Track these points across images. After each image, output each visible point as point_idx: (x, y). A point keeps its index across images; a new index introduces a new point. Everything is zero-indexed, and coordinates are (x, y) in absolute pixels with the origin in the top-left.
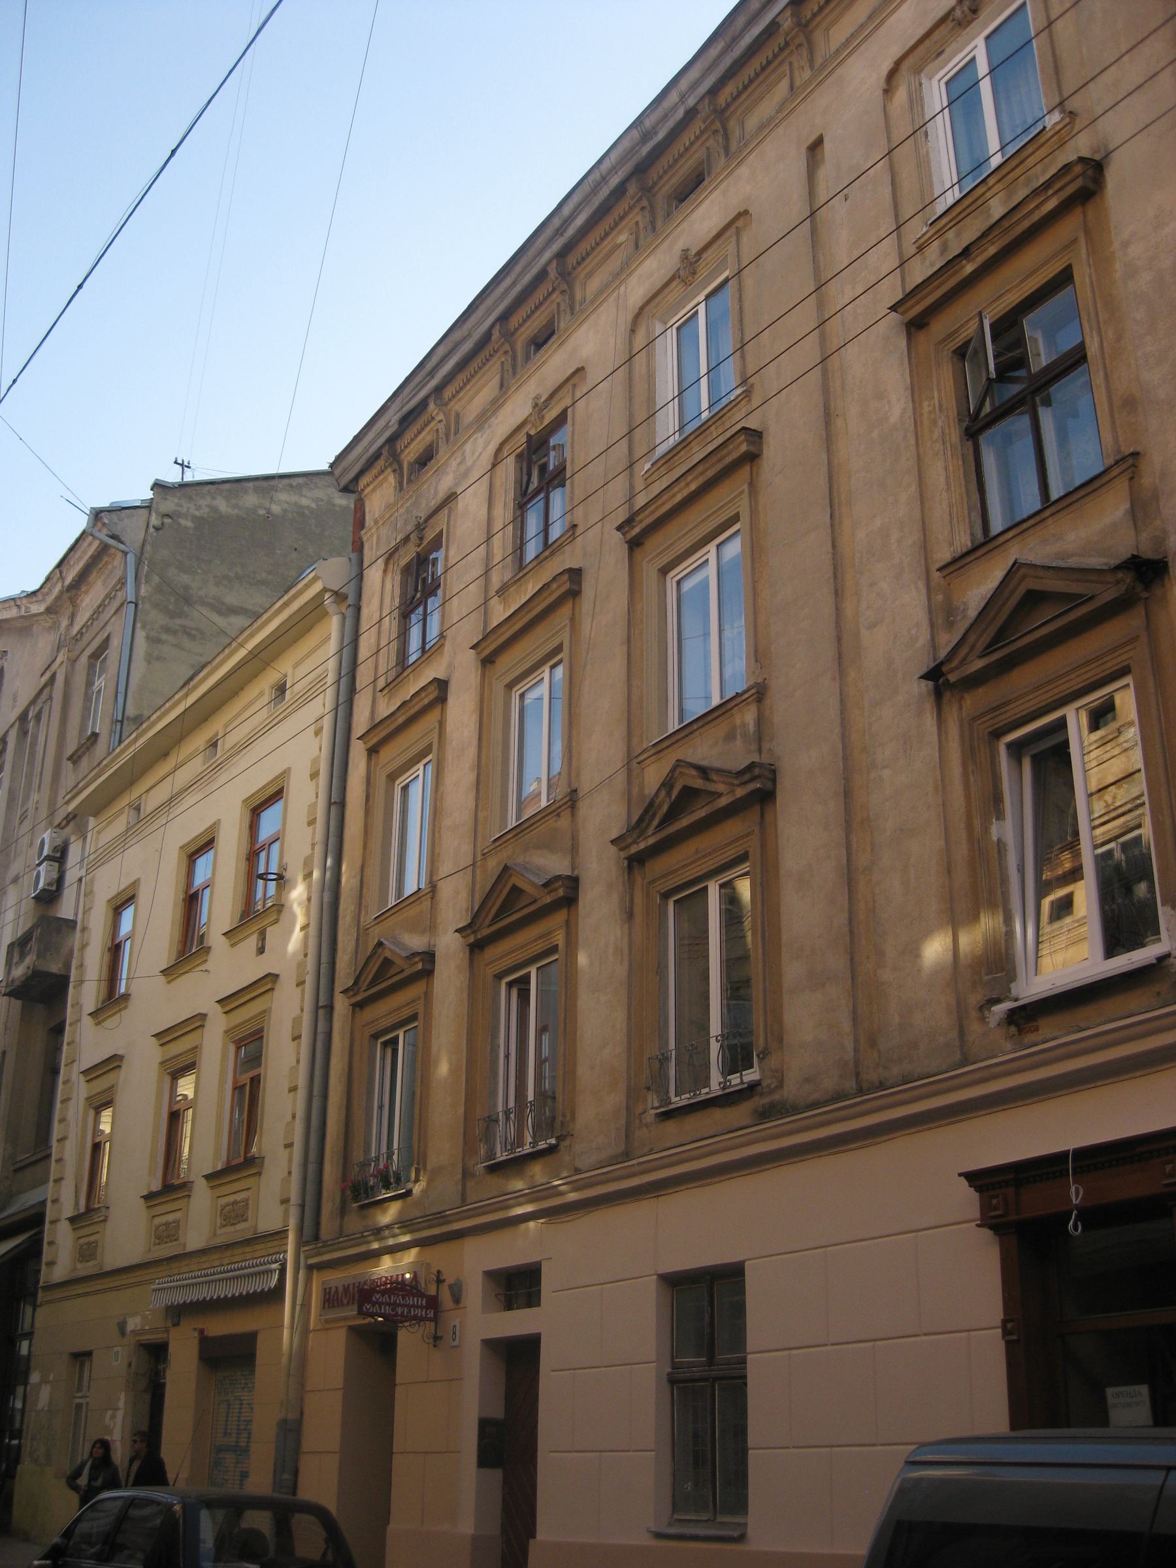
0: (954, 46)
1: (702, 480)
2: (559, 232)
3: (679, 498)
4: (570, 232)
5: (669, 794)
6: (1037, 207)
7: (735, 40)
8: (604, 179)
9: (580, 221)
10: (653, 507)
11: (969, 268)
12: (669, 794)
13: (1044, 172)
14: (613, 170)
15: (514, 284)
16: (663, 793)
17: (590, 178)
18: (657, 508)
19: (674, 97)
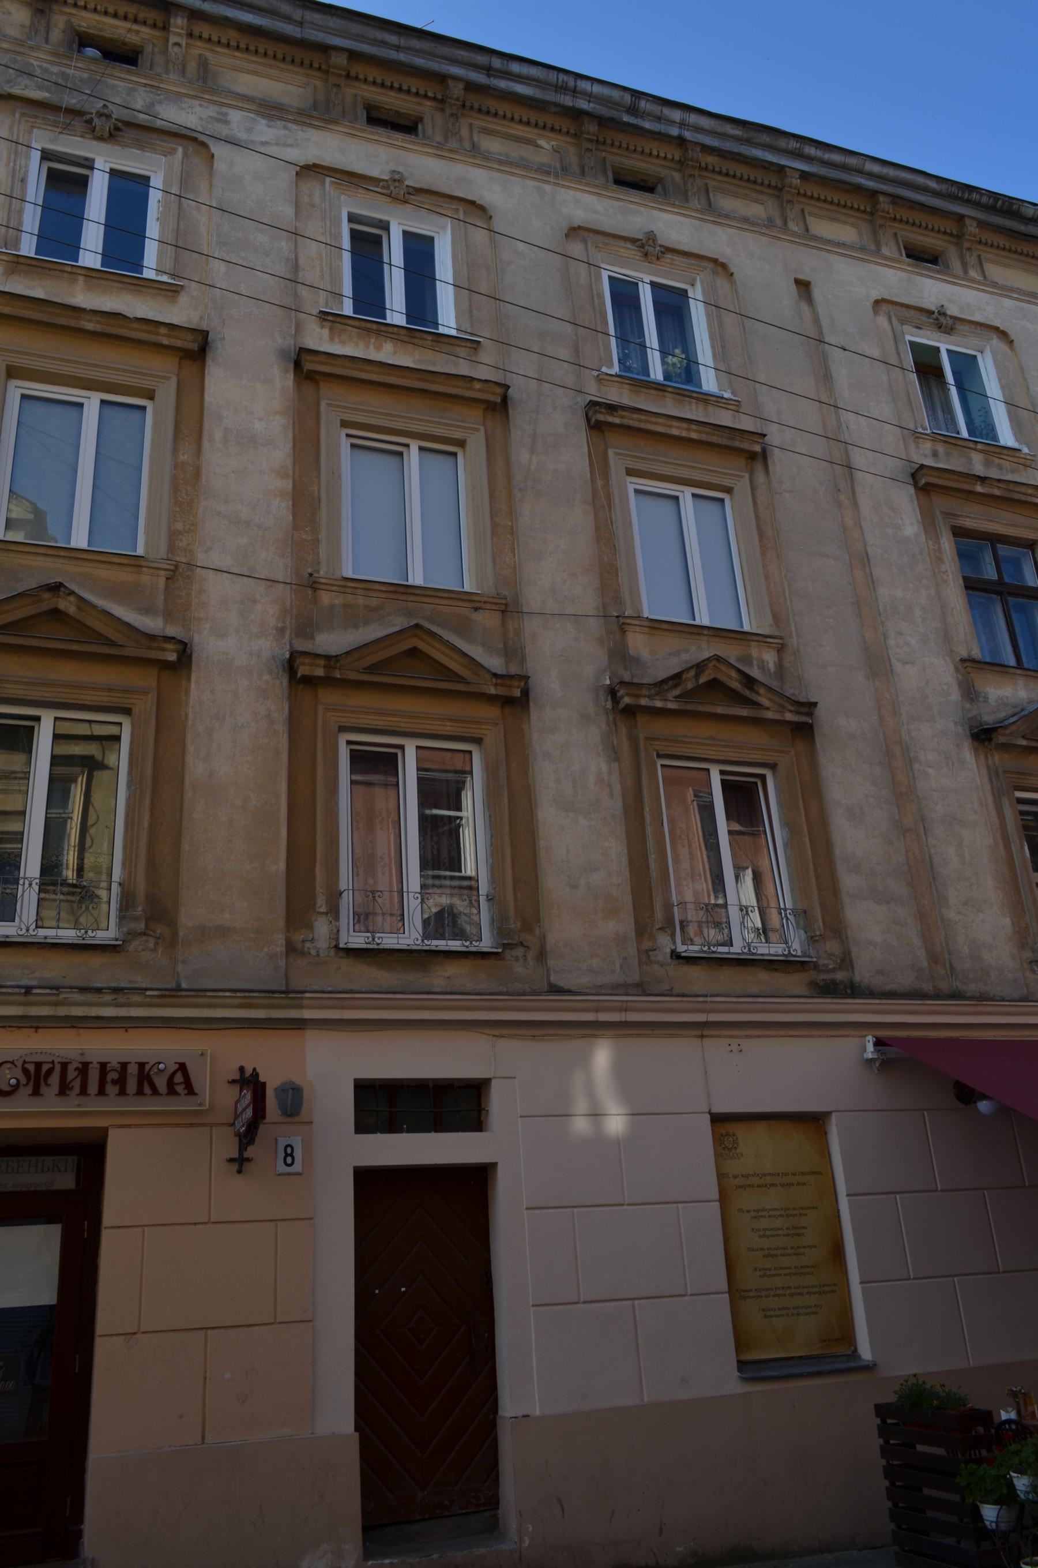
0: (929, 332)
1: (704, 437)
2: (488, 70)
3: (675, 432)
4: (502, 84)
5: (697, 676)
6: (1031, 495)
7: (748, 141)
8: (574, 92)
9: (520, 89)
10: (643, 417)
11: (979, 489)
12: (697, 676)
13: (1013, 471)
14: (589, 96)
15: (398, 48)
16: (692, 673)
17: (562, 77)
18: (647, 421)
19: (677, 115)
